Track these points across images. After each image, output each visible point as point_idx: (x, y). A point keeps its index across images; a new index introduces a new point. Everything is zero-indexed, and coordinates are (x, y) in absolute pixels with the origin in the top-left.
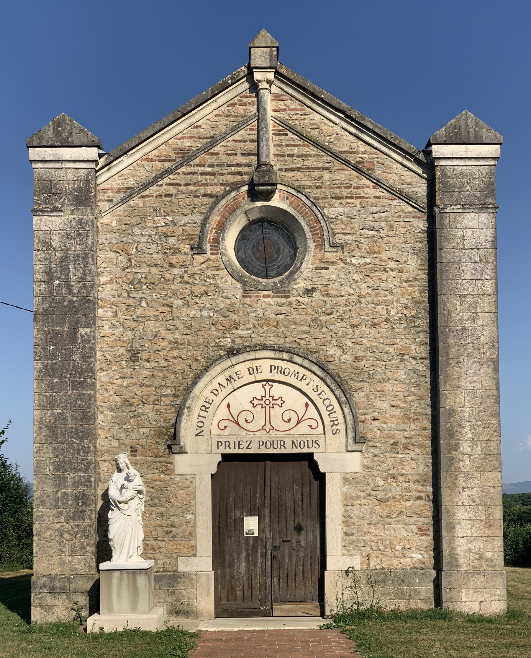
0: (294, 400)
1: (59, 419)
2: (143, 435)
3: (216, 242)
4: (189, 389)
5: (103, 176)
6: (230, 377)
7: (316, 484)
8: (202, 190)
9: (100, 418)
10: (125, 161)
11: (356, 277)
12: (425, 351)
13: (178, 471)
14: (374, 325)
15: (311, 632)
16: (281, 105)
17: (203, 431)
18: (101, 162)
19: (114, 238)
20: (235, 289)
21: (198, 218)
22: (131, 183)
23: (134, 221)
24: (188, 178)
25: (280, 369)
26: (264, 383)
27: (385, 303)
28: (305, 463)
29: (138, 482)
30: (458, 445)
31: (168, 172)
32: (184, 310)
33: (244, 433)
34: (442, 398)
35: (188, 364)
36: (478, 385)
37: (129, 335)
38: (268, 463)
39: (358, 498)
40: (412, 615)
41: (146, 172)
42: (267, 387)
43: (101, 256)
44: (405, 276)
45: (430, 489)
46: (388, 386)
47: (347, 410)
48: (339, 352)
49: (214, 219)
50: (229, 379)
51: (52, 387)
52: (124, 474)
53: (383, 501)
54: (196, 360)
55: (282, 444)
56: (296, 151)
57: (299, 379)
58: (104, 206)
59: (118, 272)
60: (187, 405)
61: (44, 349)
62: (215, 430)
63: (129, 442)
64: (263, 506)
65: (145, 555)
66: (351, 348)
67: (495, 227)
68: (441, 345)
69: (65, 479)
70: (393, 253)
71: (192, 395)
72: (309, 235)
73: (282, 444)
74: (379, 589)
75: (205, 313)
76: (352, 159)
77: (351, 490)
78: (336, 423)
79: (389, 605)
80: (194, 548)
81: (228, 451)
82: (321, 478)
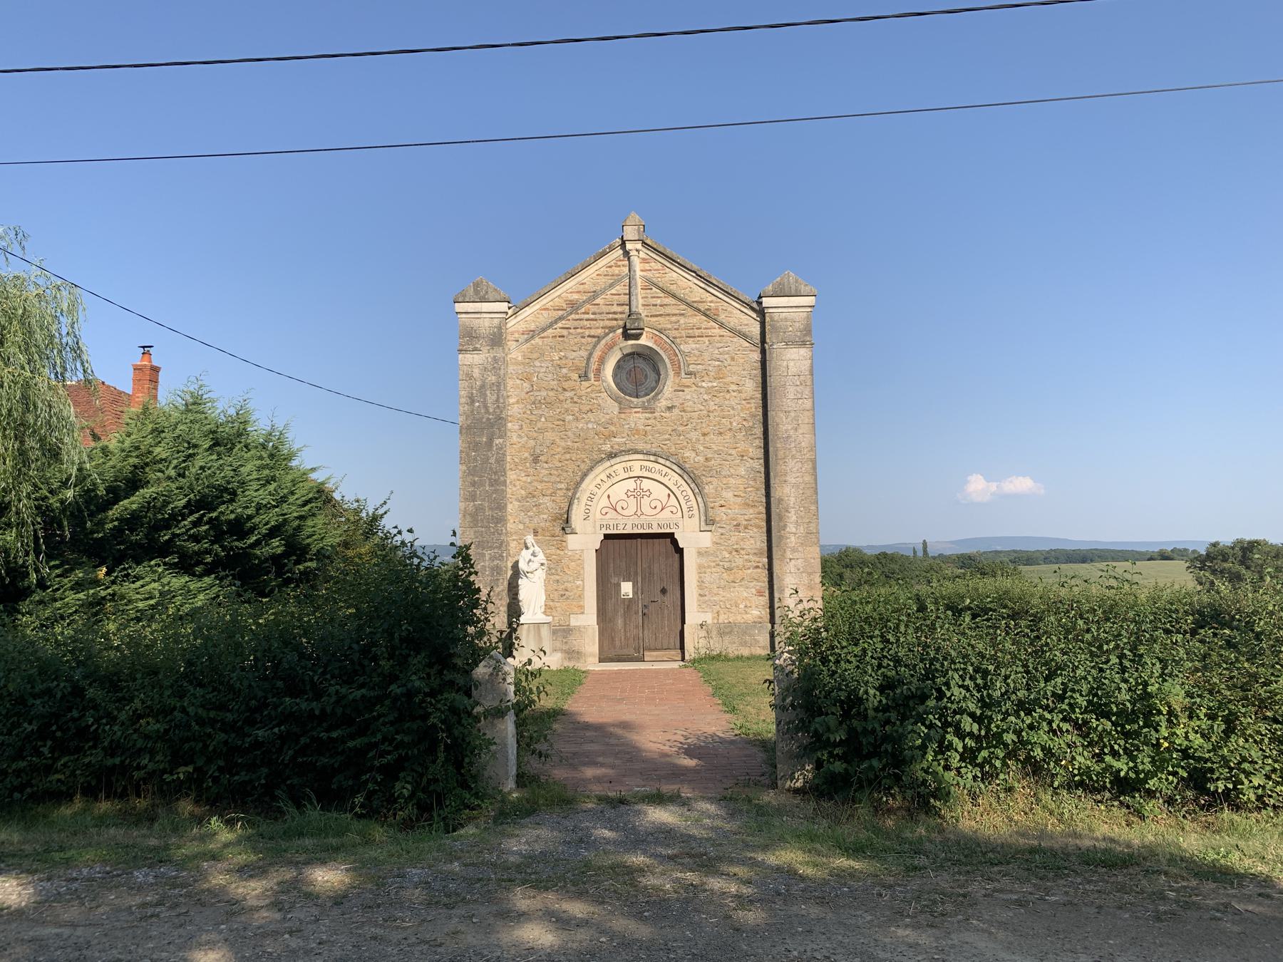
0: (659, 492)
1: (478, 509)
2: (542, 520)
3: (598, 372)
4: (578, 484)
5: (511, 322)
7: (677, 556)
8: (587, 333)
9: (510, 507)
10: (528, 311)
11: (706, 397)
12: (760, 453)
13: (570, 547)
14: (721, 433)
15: (672, 670)
16: (647, 266)
18: (510, 312)
19: (520, 369)
20: (613, 407)
21: (585, 354)
22: (533, 327)
23: (535, 356)
24: (576, 324)
27: (729, 417)
29: (541, 557)
30: (785, 526)
31: (561, 318)
32: (574, 424)
34: (772, 490)
36: (800, 480)
37: (532, 443)
39: (709, 567)
40: (751, 658)
41: (545, 318)
43: (510, 383)
44: (744, 396)
45: (766, 560)
46: (732, 481)
47: (700, 499)
49: (597, 354)
51: (473, 484)
52: (530, 551)
53: (730, 569)
55: (650, 526)
56: (658, 301)
58: (512, 345)
59: (523, 395)
61: (468, 455)
62: (598, 516)
63: (532, 526)
64: (636, 574)
65: (545, 613)
67: (812, 358)
68: (771, 449)
69: (483, 555)
70: (735, 379)
72: (669, 366)
73: (650, 526)
74: (727, 639)
75: (590, 426)
76: (702, 307)
77: (704, 561)
79: (734, 650)
80: (582, 607)
81: (609, 532)
82: (680, 551)
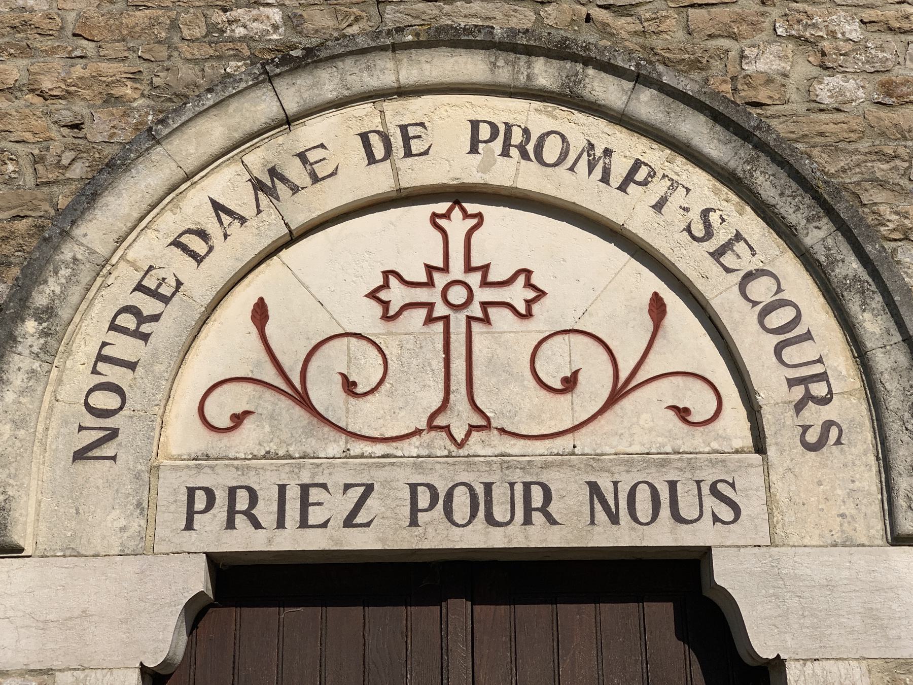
0: (592, 283)
6: (273, 172)
17: (114, 433)
25: (517, 137)
26: (442, 207)
28: (661, 614)
33: (335, 446)
35: (67, 116)
38: (459, 609)
42: (457, 226)
48: (802, 68)
50: (266, 186)
54: (110, 100)
57: (616, 179)
60: (40, 299)
62: (181, 434)
66: (859, 46)
71: (68, 252)
73: (536, 502)
78: (819, 389)
81: (244, 540)
